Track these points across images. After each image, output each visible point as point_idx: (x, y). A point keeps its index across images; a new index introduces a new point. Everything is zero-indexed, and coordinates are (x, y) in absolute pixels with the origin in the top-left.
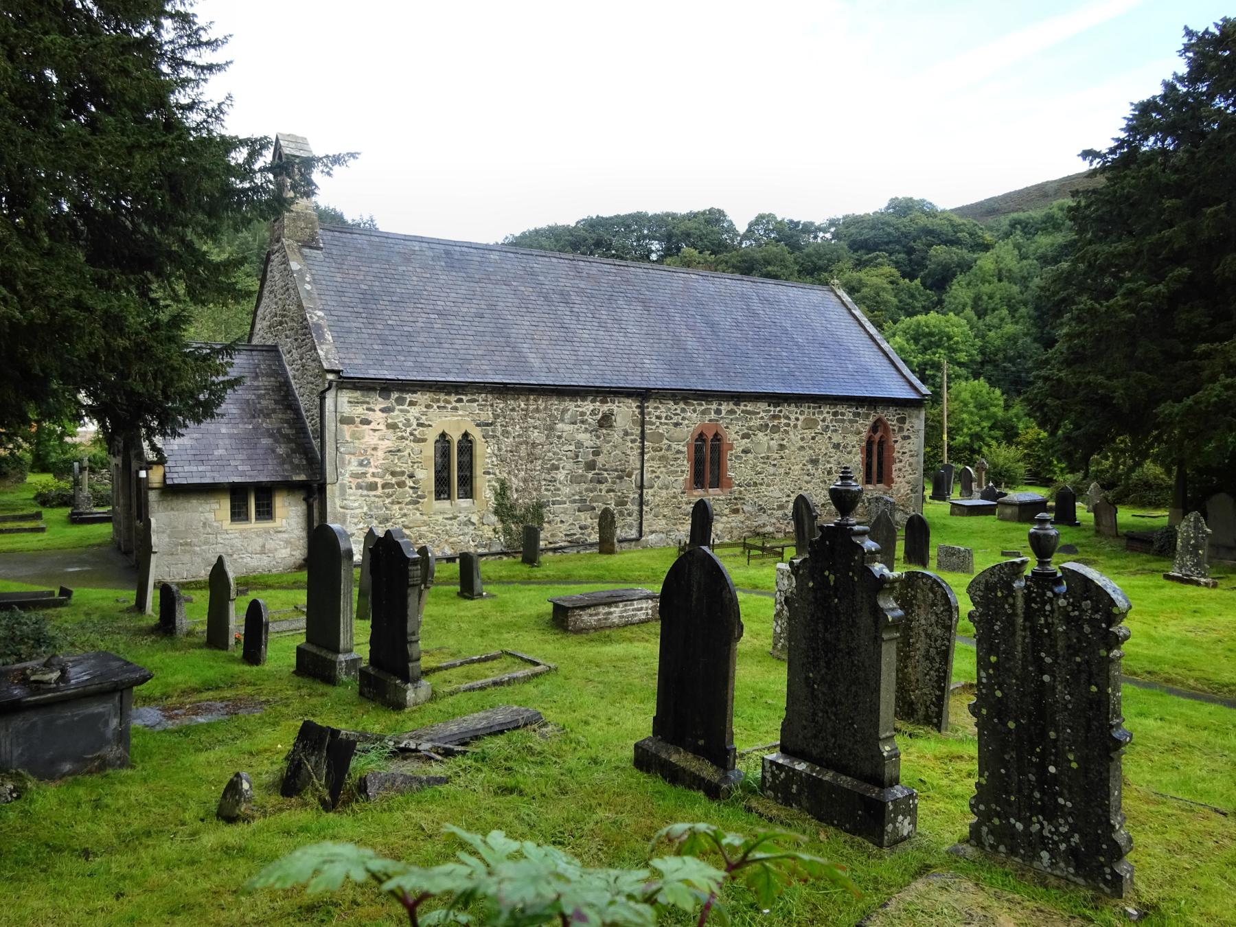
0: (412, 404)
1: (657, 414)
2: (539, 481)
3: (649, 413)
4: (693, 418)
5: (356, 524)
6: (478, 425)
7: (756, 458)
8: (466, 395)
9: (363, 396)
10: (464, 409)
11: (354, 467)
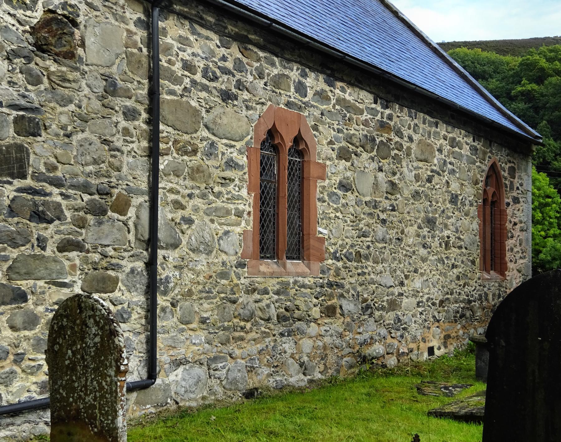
1: (185, 56)
3: (168, 49)
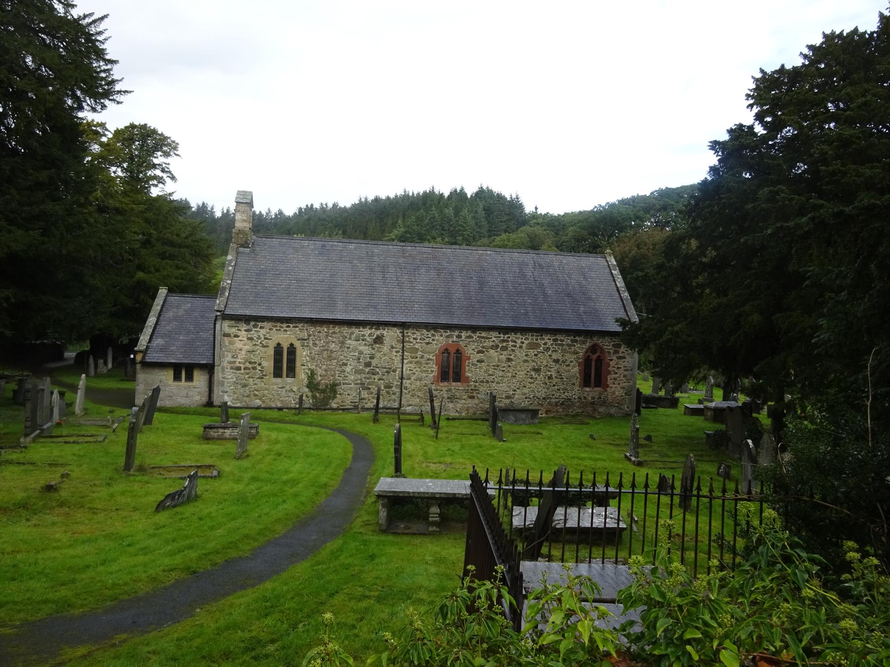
0: (261, 328)
1: (415, 336)
2: (334, 371)
3: (408, 336)
4: (440, 340)
5: (229, 387)
6: (298, 340)
8: (292, 324)
9: (235, 323)
10: (291, 331)
11: (229, 358)
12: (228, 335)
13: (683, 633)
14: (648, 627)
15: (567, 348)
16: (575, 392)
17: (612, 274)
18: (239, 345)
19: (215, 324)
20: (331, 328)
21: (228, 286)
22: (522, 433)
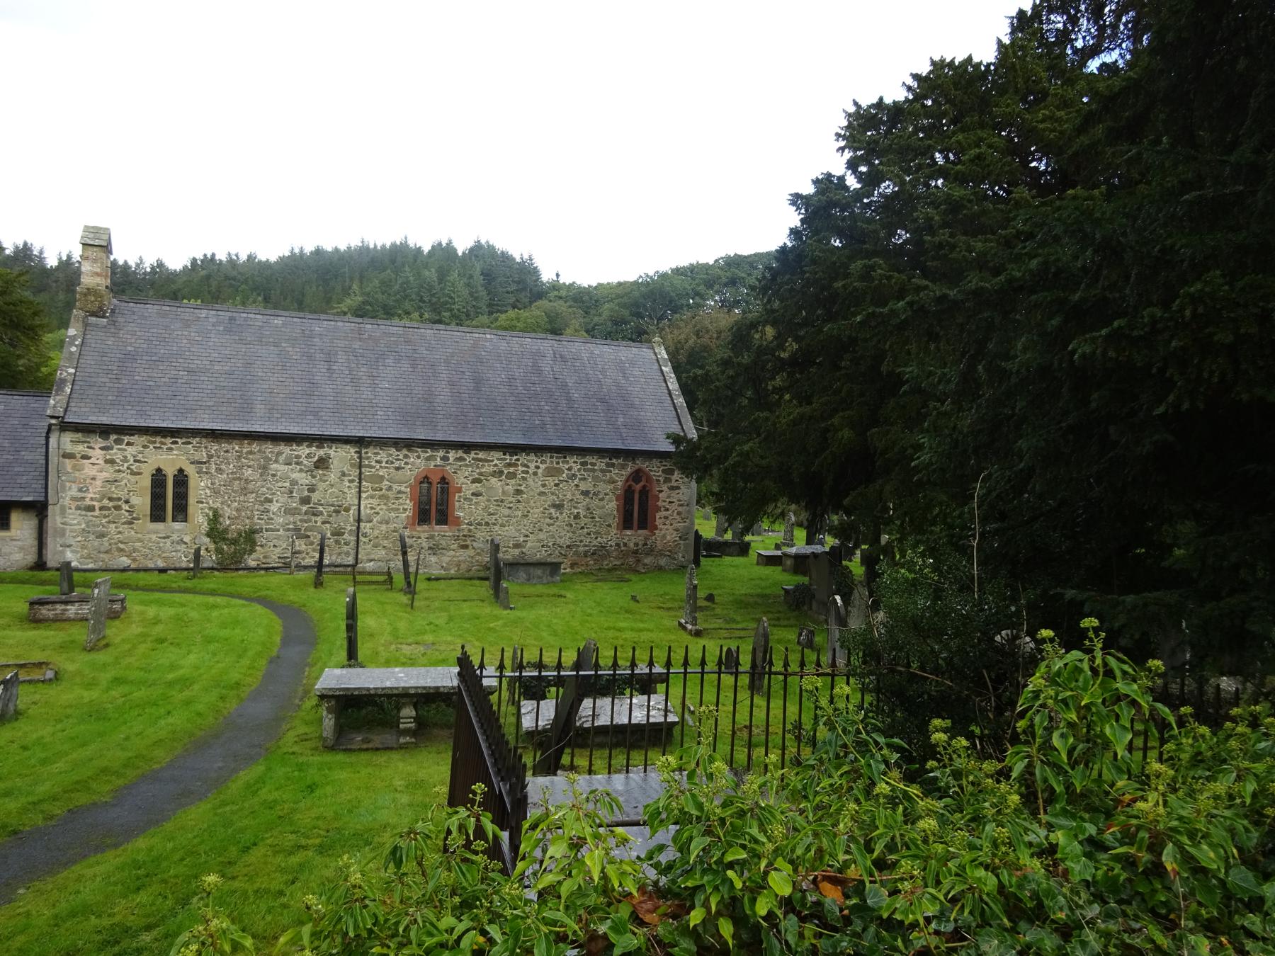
0: (129, 444)
1: (378, 458)
3: (368, 458)
4: (417, 463)
5: (74, 537)
6: (192, 463)
7: (489, 501)
10: (178, 449)
11: (74, 492)
12: (70, 456)
13: (723, 854)
14: (681, 850)
15: (600, 474)
16: (612, 536)
17: (662, 371)
18: (89, 470)
19: (47, 438)
20: (246, 446)
21: (70, 378)
22: (538, 596)
